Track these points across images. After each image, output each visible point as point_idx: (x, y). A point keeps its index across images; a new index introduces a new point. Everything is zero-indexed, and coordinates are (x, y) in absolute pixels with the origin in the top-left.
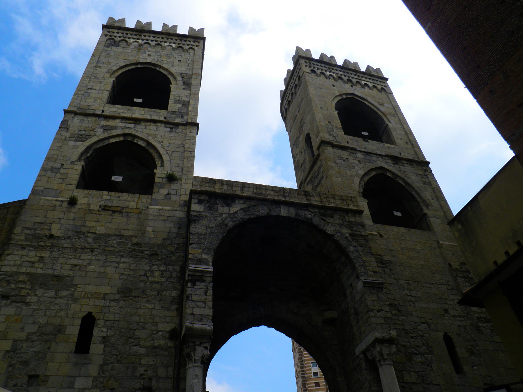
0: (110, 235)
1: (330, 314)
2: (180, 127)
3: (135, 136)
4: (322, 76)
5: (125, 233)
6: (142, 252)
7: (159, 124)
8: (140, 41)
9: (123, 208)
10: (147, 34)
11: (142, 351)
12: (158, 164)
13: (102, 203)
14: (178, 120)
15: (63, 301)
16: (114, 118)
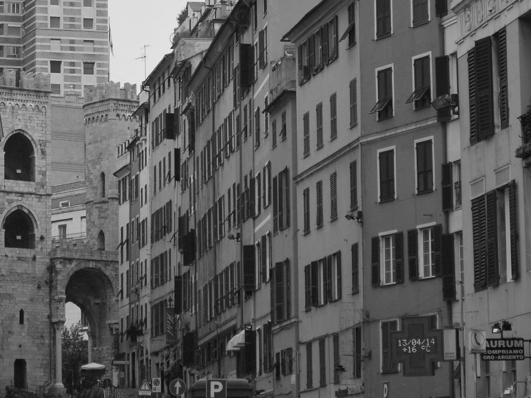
0: (23, 273)
1: (98, 301)
2: (43, 197)
3: (22, 206)
4: (123, 118)
5: (28, 272)
6: (35, 281)
7: (33, 196)
8: (12, 103)
9: (26, 258)
10: (15, 92)
11: (39, 323)
12: (35, 227)
13: (17, 256)
14: (42, 192)
15: (12, 304)
16: (11, 192)
